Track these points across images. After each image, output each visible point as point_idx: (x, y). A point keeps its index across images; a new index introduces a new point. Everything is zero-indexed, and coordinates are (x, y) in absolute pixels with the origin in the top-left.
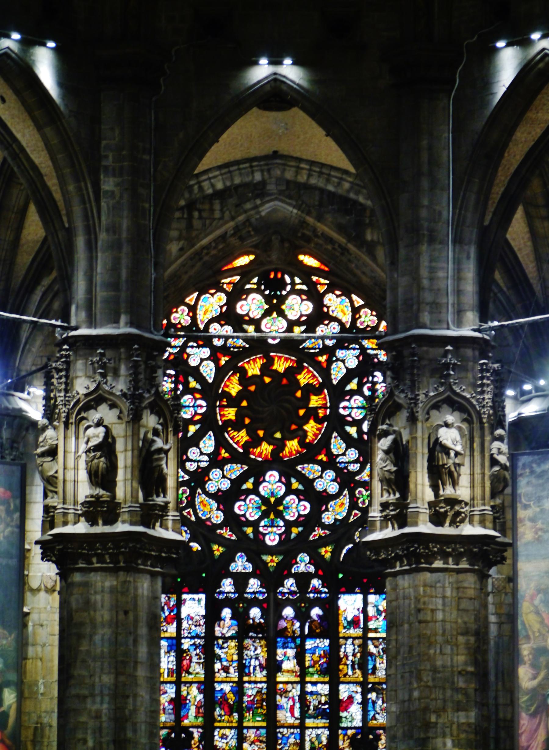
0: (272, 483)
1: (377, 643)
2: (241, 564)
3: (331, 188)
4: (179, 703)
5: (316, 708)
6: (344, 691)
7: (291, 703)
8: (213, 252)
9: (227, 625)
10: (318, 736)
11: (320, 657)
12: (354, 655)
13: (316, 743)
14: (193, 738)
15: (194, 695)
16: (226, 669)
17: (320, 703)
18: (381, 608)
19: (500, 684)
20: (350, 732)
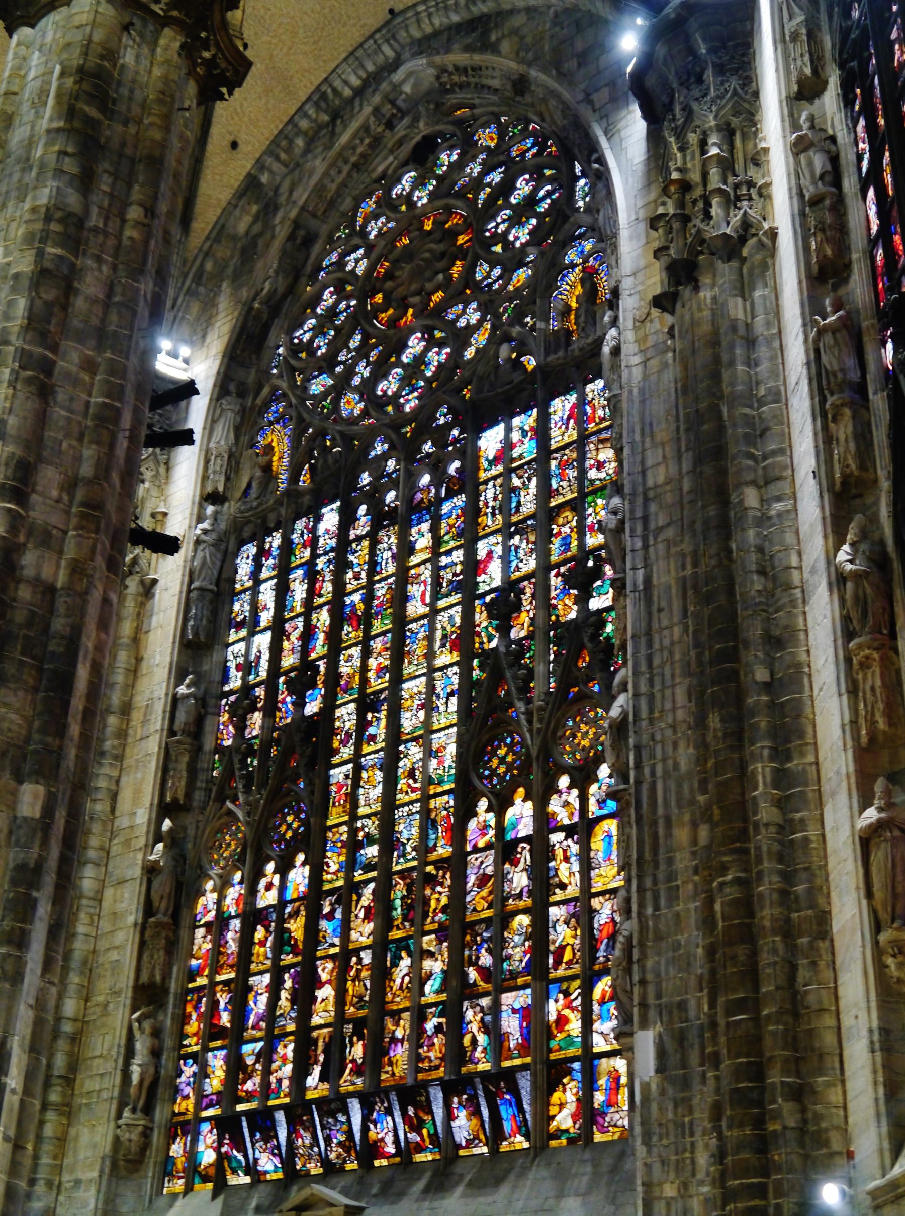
0: (415, 345)
1: (520, 472)
2: (380, 448)
3: (455, 18)
4: (308, 635)
5: (450, 582)
6: (482, 548)
7: (422, 588)
8: (360, 150)
9: (362, 526)
10: (451, 618)
11: (458, 517)
12: (495, 499)
13: (449, 628)
14: (318, 672)
15: (323, 618)
16: (357, 577)
17: (455, 574)
18: (527, 428)
19: (648, 440)
20: (488, 599)
